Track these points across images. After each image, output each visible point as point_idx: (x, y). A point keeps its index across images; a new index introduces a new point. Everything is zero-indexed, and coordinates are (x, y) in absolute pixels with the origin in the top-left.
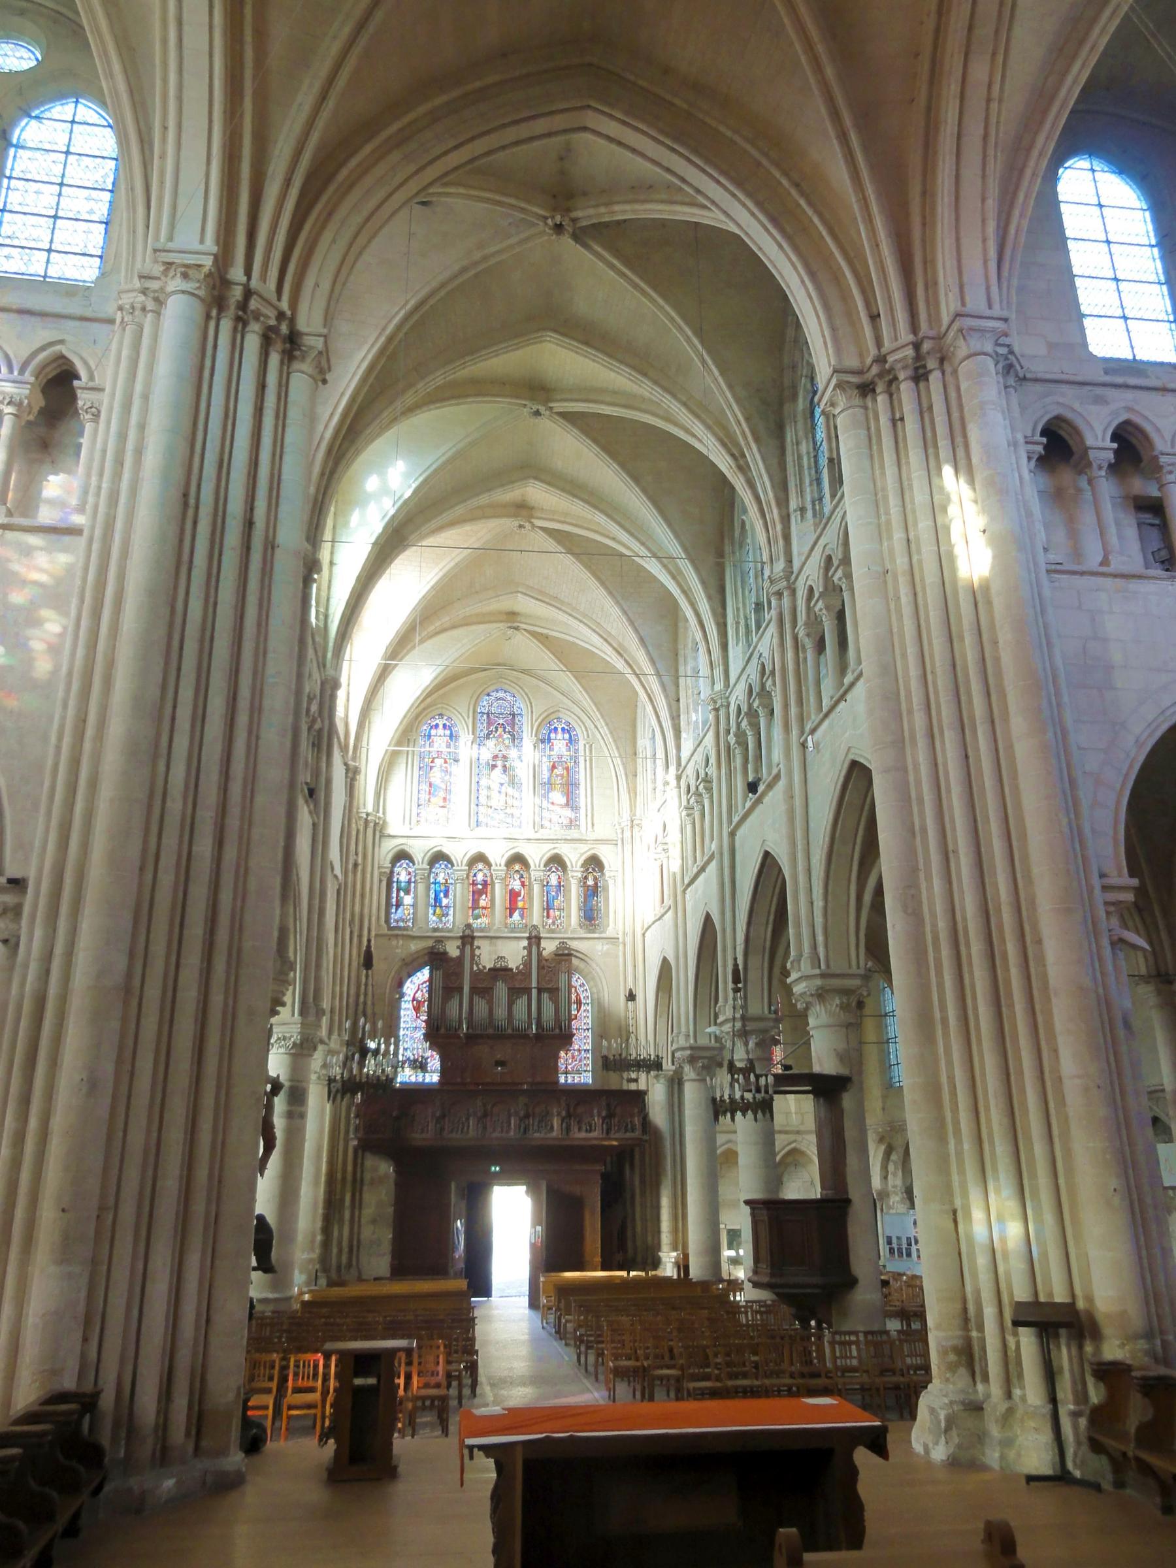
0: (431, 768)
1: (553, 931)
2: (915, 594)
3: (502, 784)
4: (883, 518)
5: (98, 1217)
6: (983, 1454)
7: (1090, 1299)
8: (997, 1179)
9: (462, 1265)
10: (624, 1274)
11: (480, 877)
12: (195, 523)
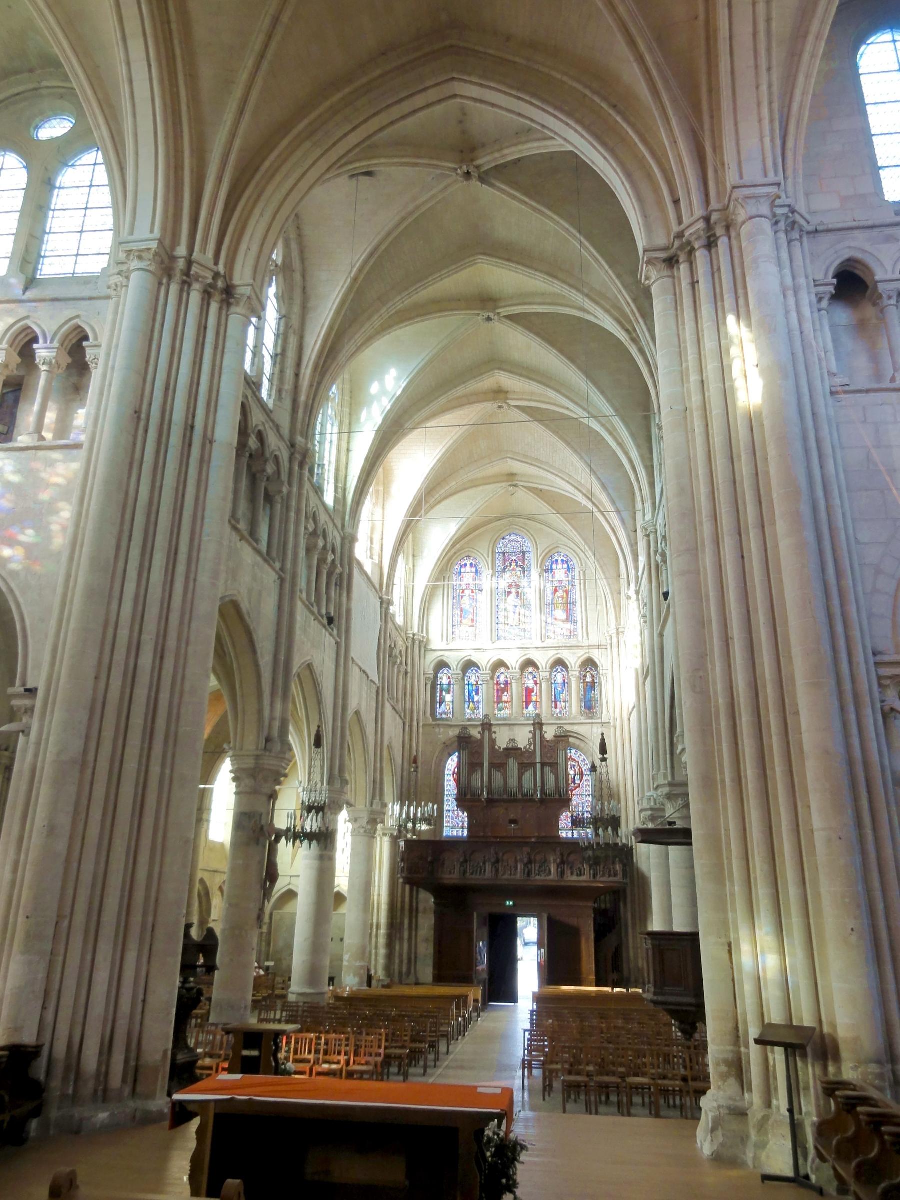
1: (560, 719)
2: (707, 426)
3: (516, 607)
4: (684, 366)
5: (57, 923)
6: (745, 1154)
7: (834, 1026)
8: (759, 916)
9: (485, 976)
10: (609, 990)
11: (502, 679)
12: (146, 431)
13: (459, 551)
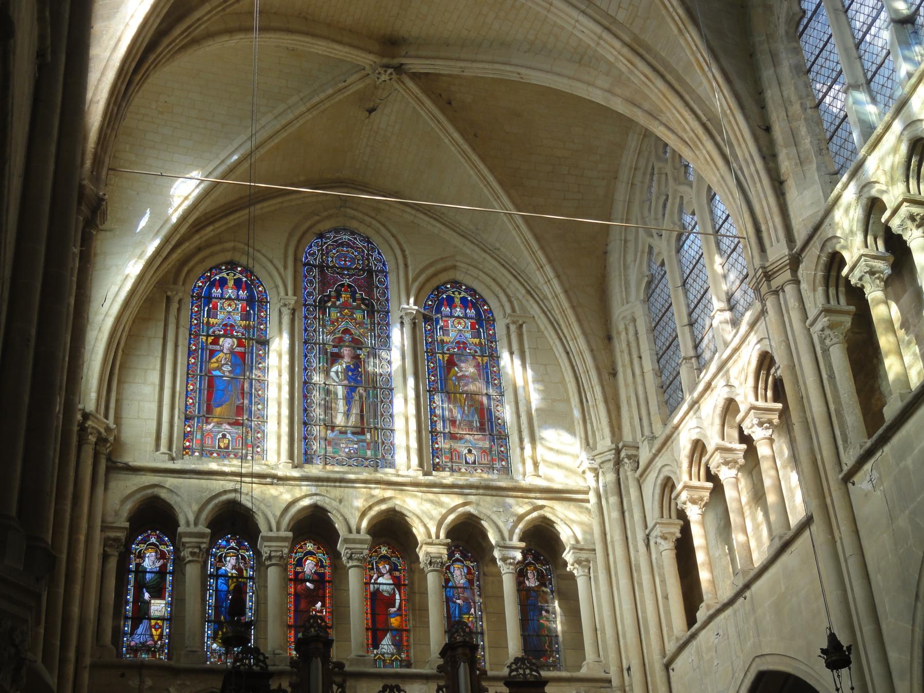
0: (212, 353)
11: (309, 566)
13: (208, 244)
